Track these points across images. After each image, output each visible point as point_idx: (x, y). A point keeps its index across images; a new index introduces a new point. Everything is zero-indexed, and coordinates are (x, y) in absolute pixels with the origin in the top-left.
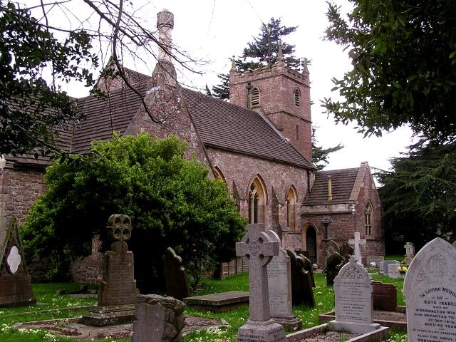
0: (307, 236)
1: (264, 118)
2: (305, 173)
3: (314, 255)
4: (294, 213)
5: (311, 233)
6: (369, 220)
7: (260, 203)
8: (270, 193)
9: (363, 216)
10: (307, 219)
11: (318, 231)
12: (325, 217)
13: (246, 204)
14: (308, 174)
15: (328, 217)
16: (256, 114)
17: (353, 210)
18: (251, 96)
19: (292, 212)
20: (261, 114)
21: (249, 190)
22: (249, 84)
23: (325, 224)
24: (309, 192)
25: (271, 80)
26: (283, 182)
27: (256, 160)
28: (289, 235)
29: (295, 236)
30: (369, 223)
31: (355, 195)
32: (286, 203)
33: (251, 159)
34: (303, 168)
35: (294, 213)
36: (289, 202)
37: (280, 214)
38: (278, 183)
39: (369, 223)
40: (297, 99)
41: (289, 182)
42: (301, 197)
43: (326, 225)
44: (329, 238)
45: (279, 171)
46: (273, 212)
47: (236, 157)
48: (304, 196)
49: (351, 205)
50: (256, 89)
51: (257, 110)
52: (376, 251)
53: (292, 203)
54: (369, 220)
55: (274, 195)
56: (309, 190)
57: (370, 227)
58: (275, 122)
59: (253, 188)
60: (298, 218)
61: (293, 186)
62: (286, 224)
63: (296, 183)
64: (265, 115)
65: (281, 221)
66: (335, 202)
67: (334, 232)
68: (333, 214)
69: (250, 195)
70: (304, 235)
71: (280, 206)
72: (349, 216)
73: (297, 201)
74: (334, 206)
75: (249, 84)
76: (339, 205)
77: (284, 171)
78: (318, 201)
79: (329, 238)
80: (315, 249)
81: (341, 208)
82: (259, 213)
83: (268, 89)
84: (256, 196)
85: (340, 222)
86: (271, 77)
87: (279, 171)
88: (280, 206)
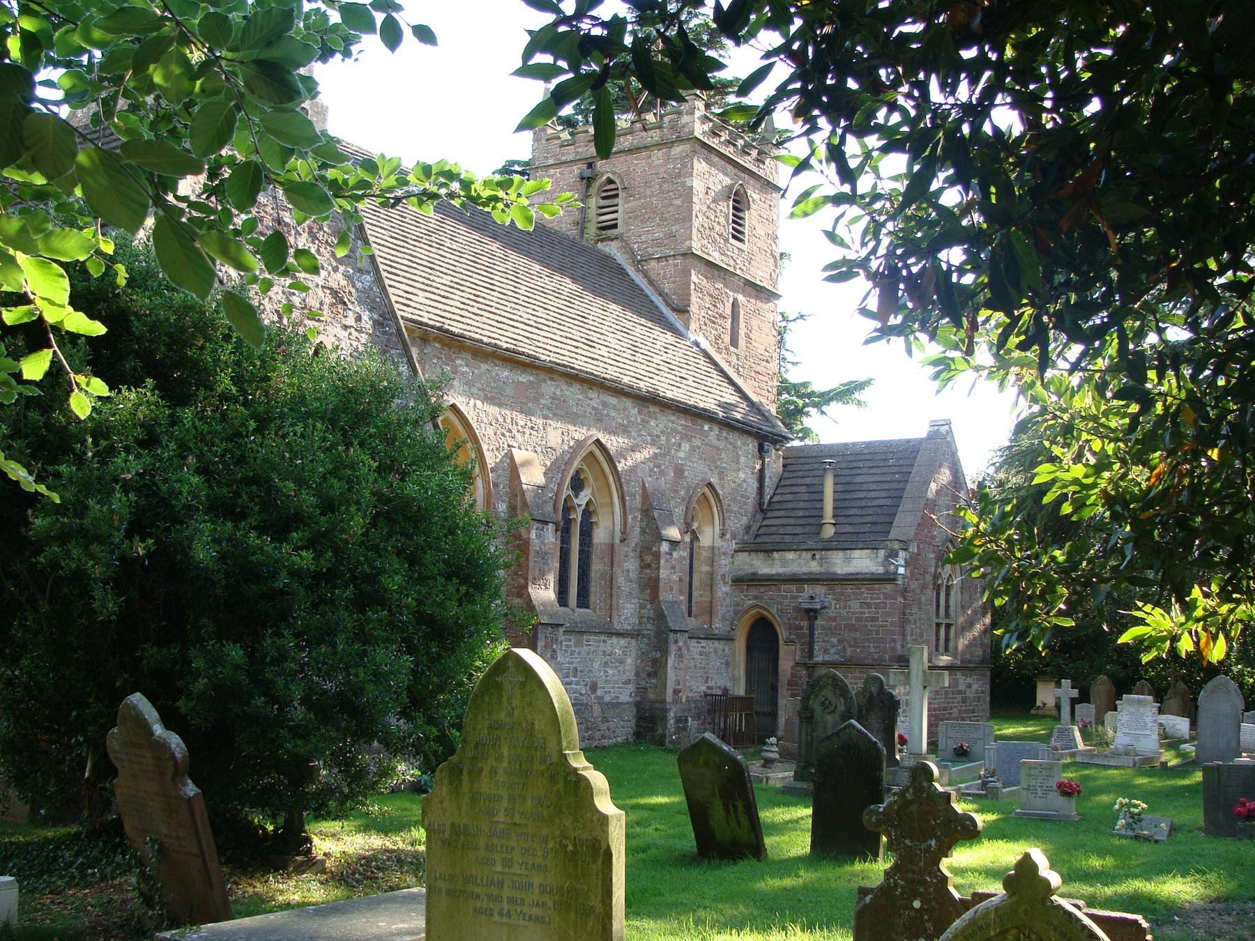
0: (750, 649)
1: (630, 270)
2: (752, 446)
3: (767, 709)
4: (711, 575)
5: (762, 637)
6: (947, 607)
7: (600, 536)
8: (636, 502)
9: (930, 592)
10: (753, 592)
11: (783, 634)
12: (808, 590)
13: (551, 536)
14: (761, 451)
15: (820, 590)
16: (608, 260)
17: (901, 570)
18: (593, 202)
19: (706, 569)
20: (621, 259)
21: (566, 492)
22: (590, 166)
23: (809, 611)
24: (762, 508)
25: (658, 156)
26: (679, 471)
27: (591, 394)
28: (693, 643)
29: (711, 646)
30: (947, 615)
31: (904, 525)
32: (687, 538)
33: (576, 387)
34: (749, 433)
35: (711, 575)
36: (695, 538)
37: (663, 573)
38: (662, 473)
39: (947, 615)
40: (738, 221)
41: (697, 471)
42: (737, 523)
43: (811, 614)
44: (819, 658)
45: (668, 436)
46: (644, 566)
47: (524, 378)
48: (745, 520)
49: (893, 554)
50: (610, 181)
51: (612, 249)
52: (964, 700)
53: (707, 538)
54: (947, 607)
55: (647, 512)
56: (761, 504)
57: (948, 626)
58: (667, 287)
59: (577, 484)
60: (723, 589)
61: (710, 485)
62: (684, 608)
63: (722, 476)
64: (637, 263)
65: (666, 596)
66: (844, 543)
67: (834, 640)
68: (832, 581)
69: (568, 509)
70: (740, 644)
71: (665, 547)
72: (888, 588)
73: (723, 535)
74: (840, 554)
75: (590, 166)
76: (857, 553)
77: (686, 437)
78: (788, 539)
79: (819, 658)
80: (774, 688)
81: (862, 562)
82: (597, 567)
83: (647, 184)
84: (588, 513)
85: (855, 605)
86: (659, 146)
87: (668, 436)
88: (665, 547)
